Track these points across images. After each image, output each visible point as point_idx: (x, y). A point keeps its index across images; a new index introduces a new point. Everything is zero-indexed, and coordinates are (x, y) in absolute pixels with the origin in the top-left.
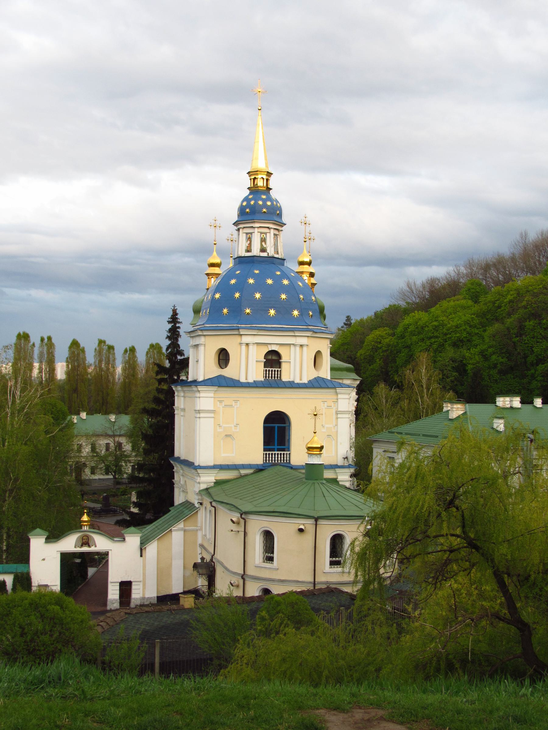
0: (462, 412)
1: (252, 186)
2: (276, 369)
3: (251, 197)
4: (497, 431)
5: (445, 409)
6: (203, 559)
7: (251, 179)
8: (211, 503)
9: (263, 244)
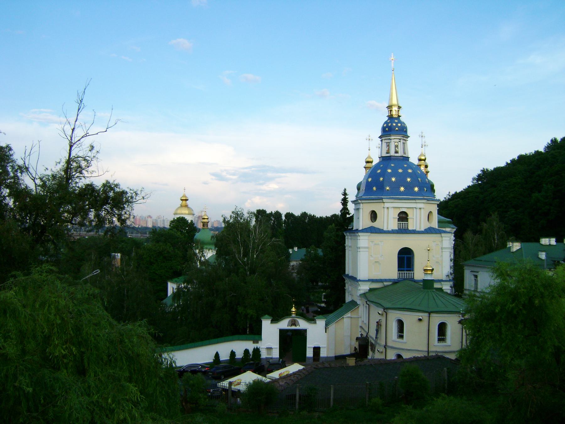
1: (389, 115)
2: (405, 223)
3: (389, 121)
5: (508, 246)
6: (362, 335)
7: (388, 111)
8: (366, 302)
9: (396, 148)
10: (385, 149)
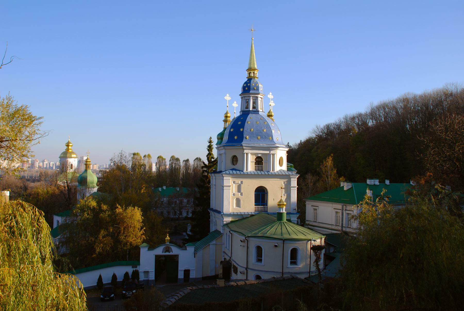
0: (350, 187)
1: (249, 76)
2: (261, 166)
3: (248, 82)
4: (163, 189)
5: (342, 185)
6: (225, 259)
7: (248, 73)
8: (230, 231)
9: (254, 104)
10: (245, 105)
